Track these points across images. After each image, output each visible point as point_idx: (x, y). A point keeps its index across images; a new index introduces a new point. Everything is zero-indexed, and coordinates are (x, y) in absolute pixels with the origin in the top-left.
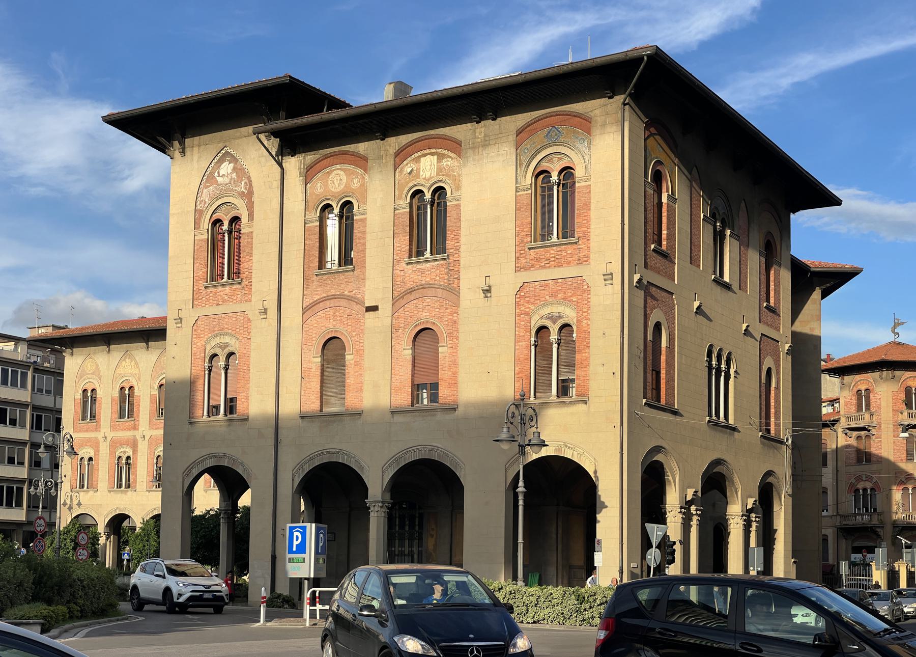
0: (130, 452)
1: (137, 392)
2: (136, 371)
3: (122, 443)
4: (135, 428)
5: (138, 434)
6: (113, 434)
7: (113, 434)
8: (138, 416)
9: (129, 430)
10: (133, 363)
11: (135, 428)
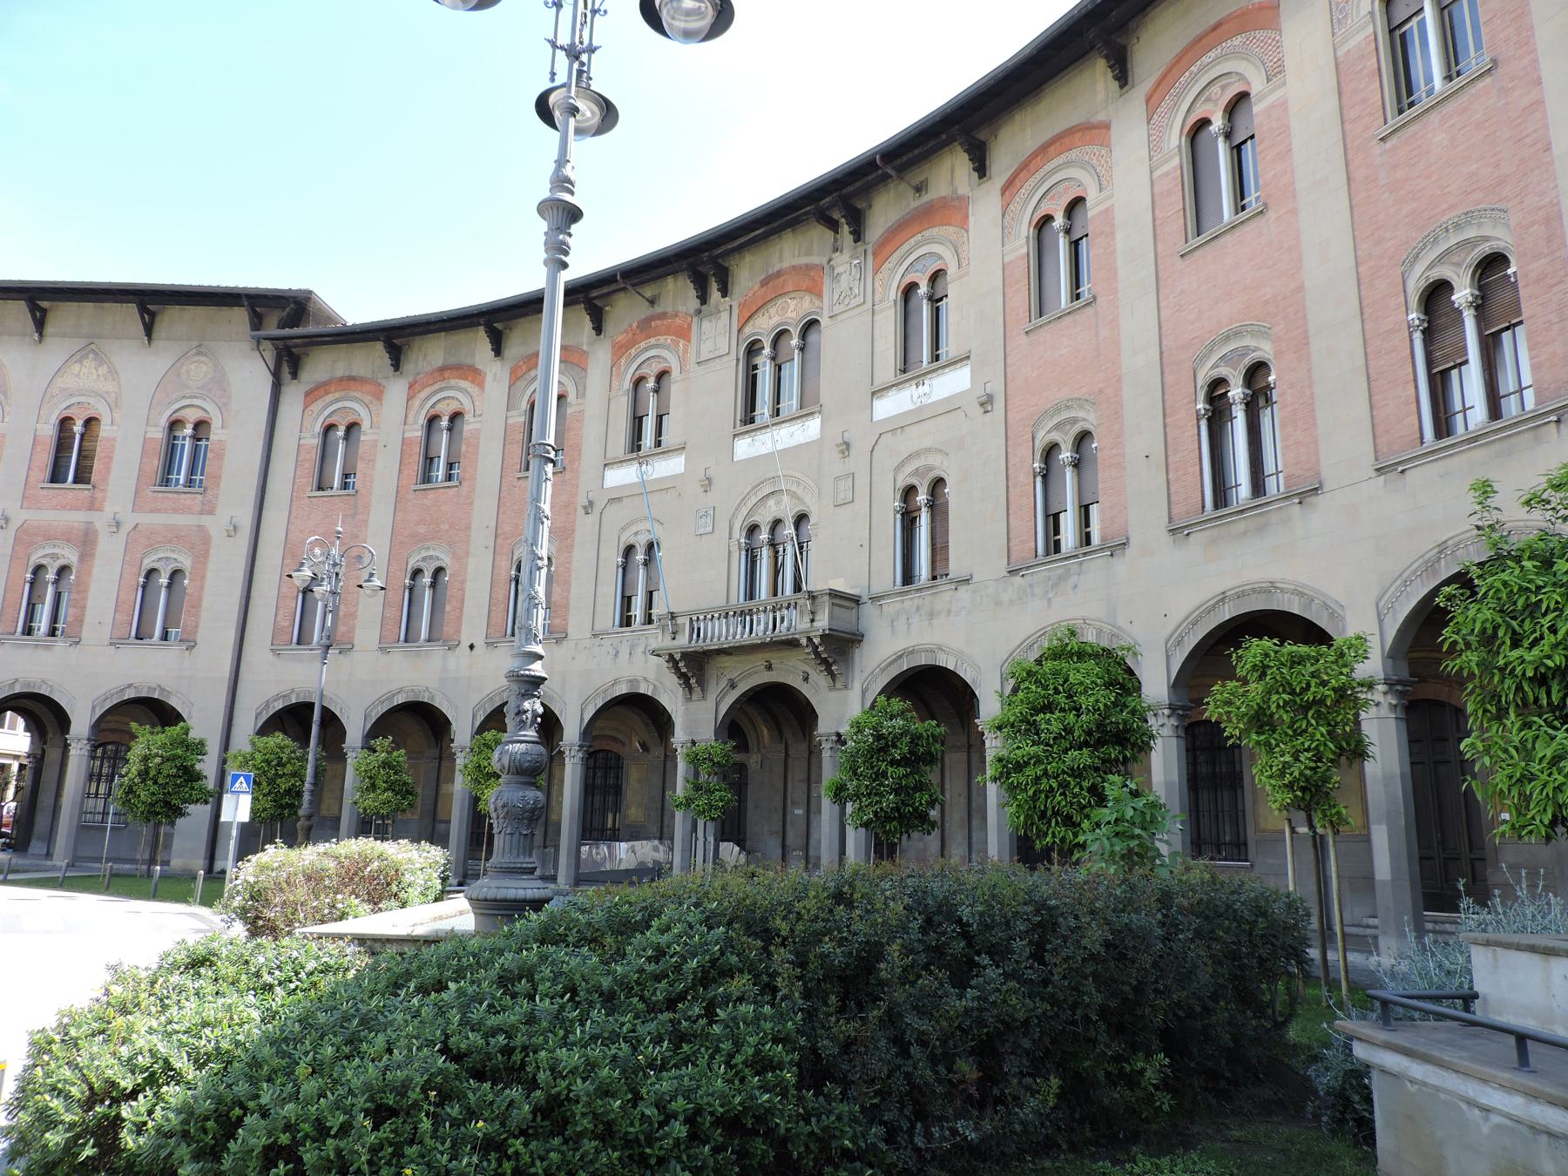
0: (70, 556)
1: (105, 430)
2: (110, 387)
3: (49, 536)
4: (92, 506)
5: (100, 521)
6: (26, 515)
7: (26, 515)
8: (105, 480)
9: (77, 509)
10: (103, 370)
11: (92, 506)
